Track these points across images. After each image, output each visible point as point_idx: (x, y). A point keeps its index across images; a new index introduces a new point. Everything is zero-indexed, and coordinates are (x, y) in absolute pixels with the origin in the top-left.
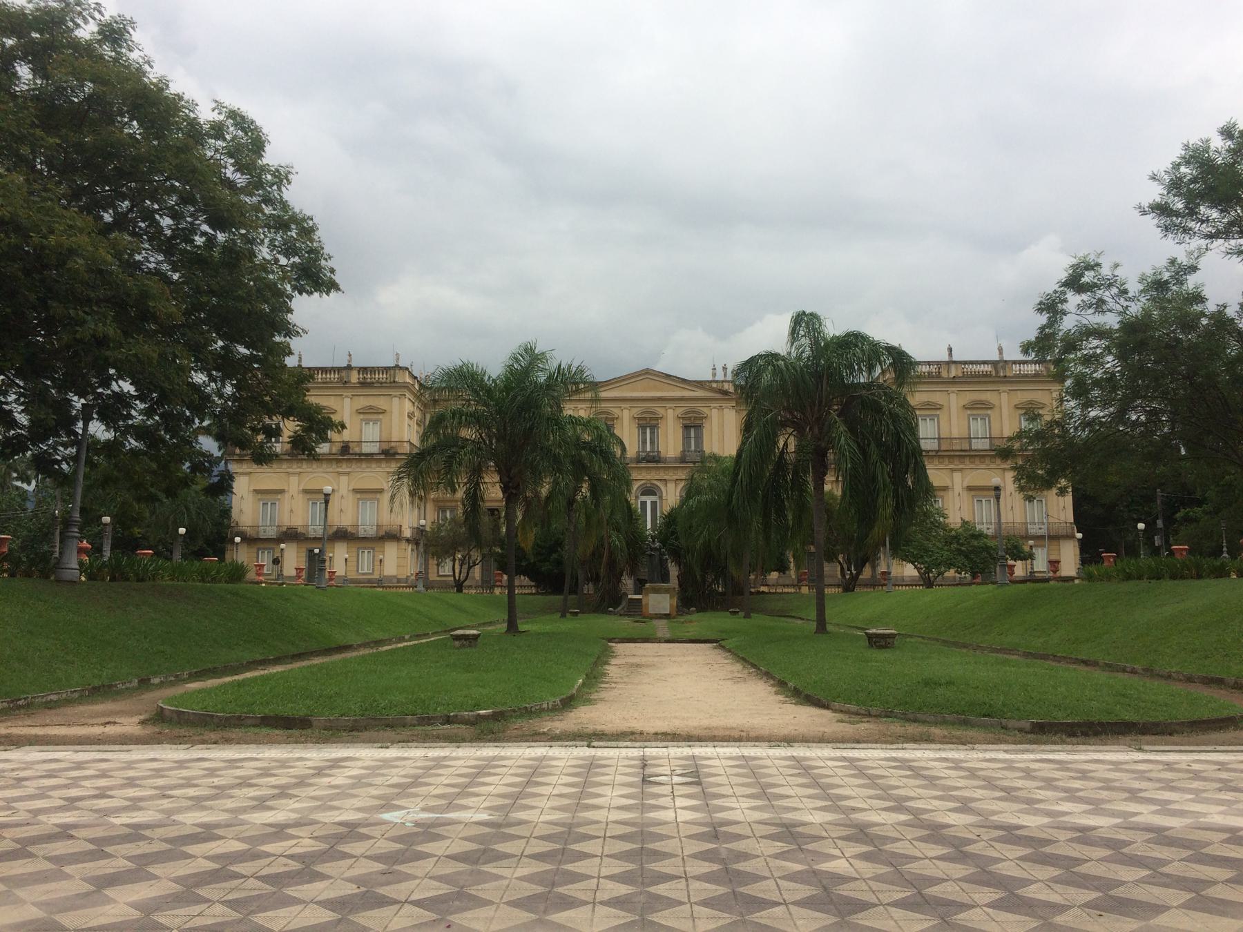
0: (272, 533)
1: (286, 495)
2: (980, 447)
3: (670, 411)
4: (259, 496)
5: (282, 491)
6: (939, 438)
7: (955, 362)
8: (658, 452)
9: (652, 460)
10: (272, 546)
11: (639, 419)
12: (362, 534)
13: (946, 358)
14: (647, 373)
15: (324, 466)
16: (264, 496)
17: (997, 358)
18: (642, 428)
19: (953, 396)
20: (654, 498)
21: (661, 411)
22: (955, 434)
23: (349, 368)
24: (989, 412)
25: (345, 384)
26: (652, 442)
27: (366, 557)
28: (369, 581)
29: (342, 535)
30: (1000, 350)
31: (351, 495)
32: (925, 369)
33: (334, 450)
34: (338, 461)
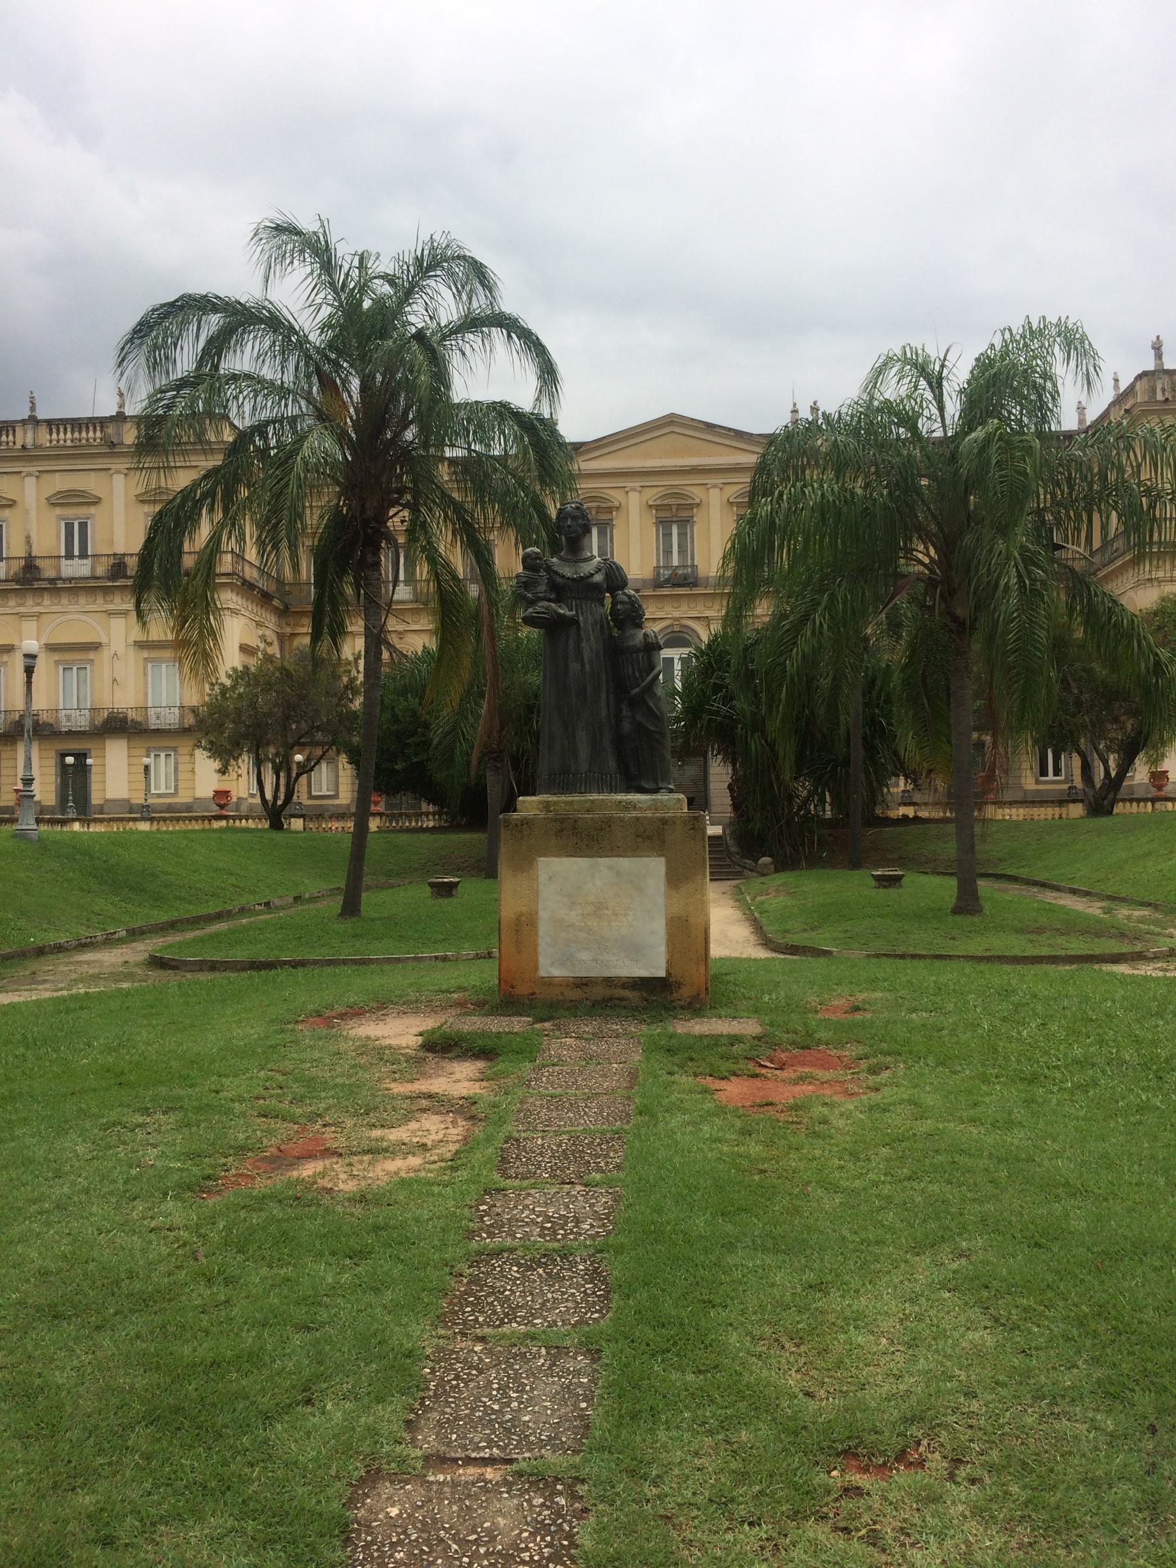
3: (714, 493)
8: (693, 566)
9: (681, 581)
11: (658, 508)
12: (153, 723)
14: (672, 422)
15: (82, 600)
18: (663, 524)
20: (685, 651)
21: (698, 493)
23: (120, 418)
25: (112, 447)
26: (682, 551)
27: (162, 767)
28: (170, 808)
29: (117, 726)
31: (132, 652)
33: (101, 571)
34: (106, 590)
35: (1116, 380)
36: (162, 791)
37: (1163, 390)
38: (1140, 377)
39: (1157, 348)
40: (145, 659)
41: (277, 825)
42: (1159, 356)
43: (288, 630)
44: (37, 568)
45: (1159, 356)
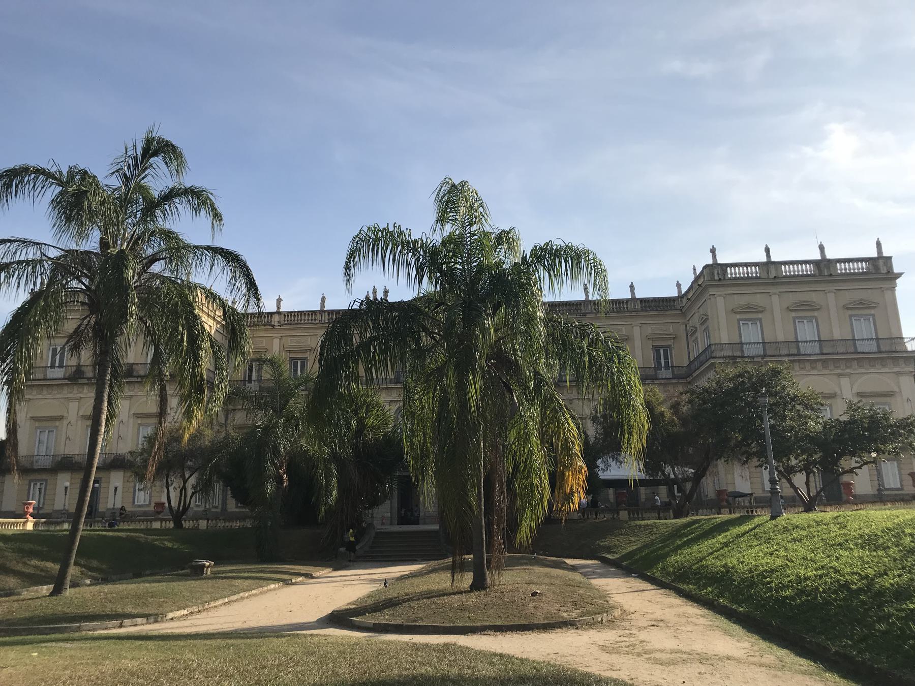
0: (47, 463)
1: (65, 422)
2: (808, 352)
4: (37, 424)
5: (61, 418)
6: (764, 343)
7: (774, 263)
10: (44, 477)
13: (764, 259)
16: (44, 424)
17: (819, 258)
19: (775, 298)
22: (781, 338)
24: (816, 314)
30: (822, 248)
32: (740, 272)
35: (695, 269)
36: (142, 503)
37: (718, 274)
38: (705, 267)
39: (713, 251)
40: (140, 425)
41: (178, 525)
42: (714, 256)
43: (231, 407)
44: (83, 372)
45: (714, 256)
